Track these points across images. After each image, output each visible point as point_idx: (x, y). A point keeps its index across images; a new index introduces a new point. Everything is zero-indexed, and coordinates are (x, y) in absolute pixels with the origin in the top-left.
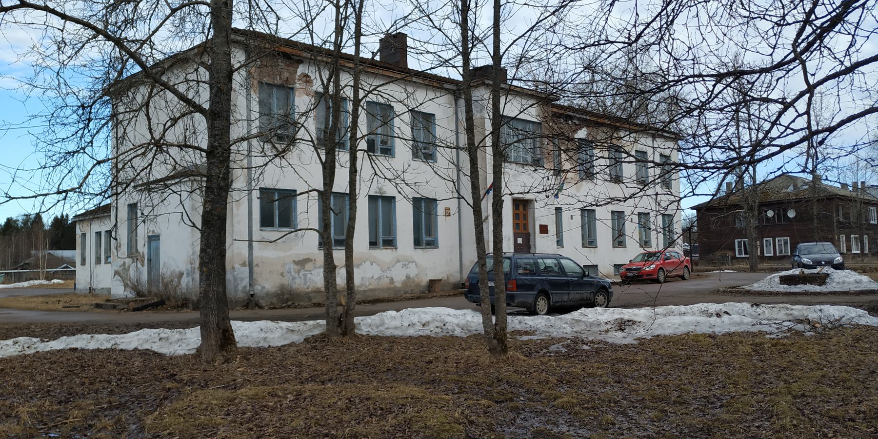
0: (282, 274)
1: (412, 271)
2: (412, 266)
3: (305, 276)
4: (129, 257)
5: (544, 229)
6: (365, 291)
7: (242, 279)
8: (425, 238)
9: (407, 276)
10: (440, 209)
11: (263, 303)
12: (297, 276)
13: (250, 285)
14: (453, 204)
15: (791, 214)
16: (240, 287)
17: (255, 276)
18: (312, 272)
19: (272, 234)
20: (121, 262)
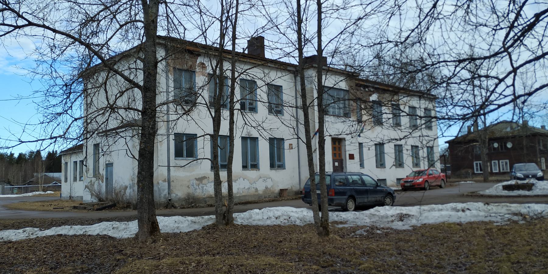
0: (188, 187)
1: (269, 184)
2: (269, 180)
3: (203, 187)
4: (94, 177)
5: (352, 157)
6: (240, 196)
7: (164, 190)
8: (277, 163)
9: (266, 187)
10: (286, 145)
11: (176, 205)
12: (198, 188)
13: (169, 194)
14: (294, 142)
15: (509, 145)
16: (162, 195)
17: (171, 188)
18: (207, 185)
19: (182, 162)
20: (89, 180)
